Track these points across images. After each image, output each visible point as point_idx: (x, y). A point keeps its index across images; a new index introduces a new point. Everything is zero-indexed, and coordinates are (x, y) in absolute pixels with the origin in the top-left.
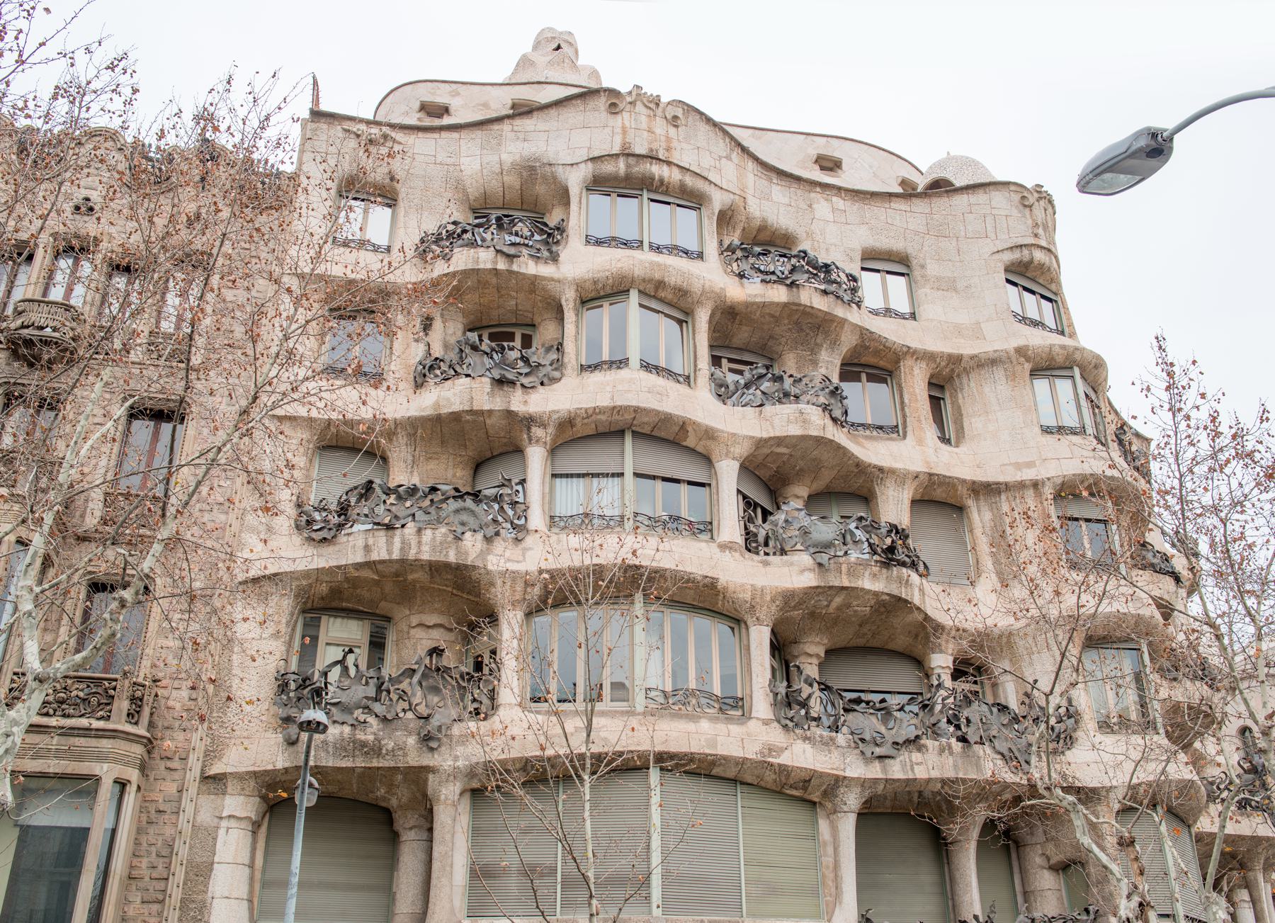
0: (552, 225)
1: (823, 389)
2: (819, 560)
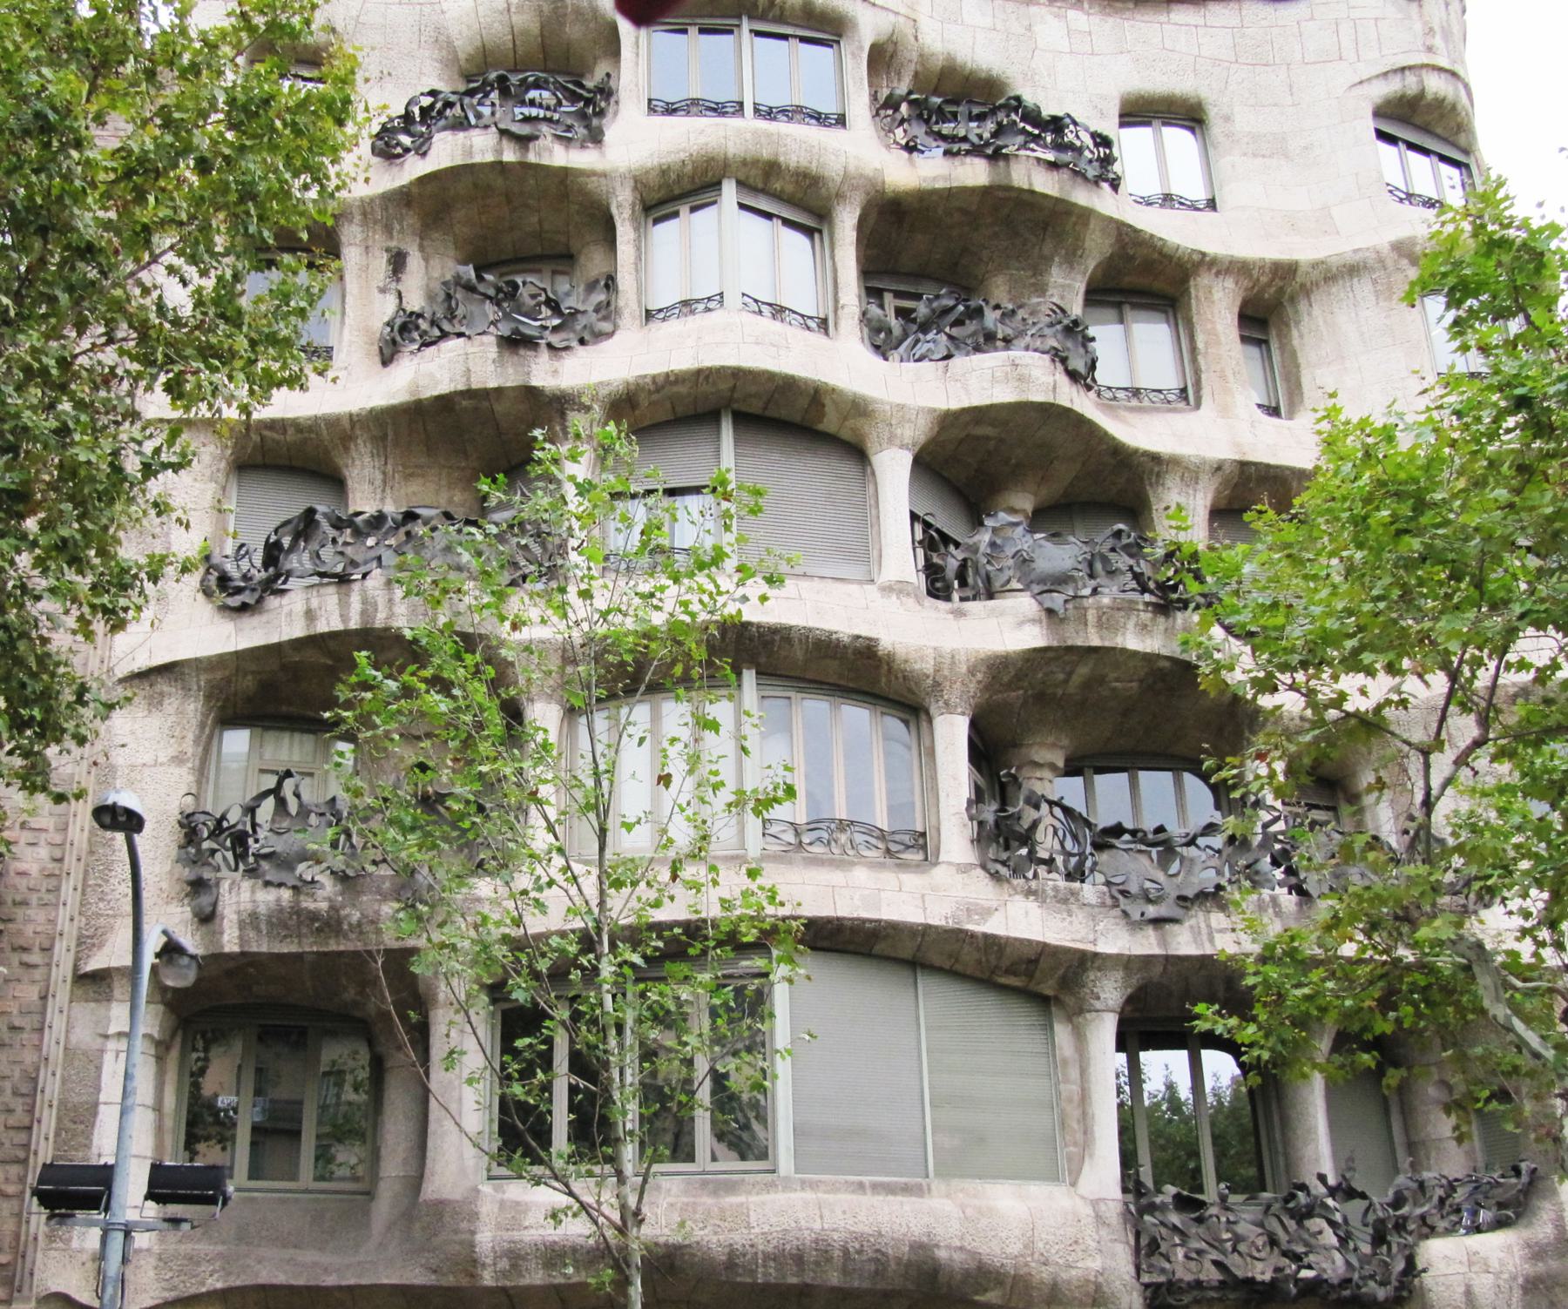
0: (589, 84)
1: (1051, 325)
2: (1048, 604)
